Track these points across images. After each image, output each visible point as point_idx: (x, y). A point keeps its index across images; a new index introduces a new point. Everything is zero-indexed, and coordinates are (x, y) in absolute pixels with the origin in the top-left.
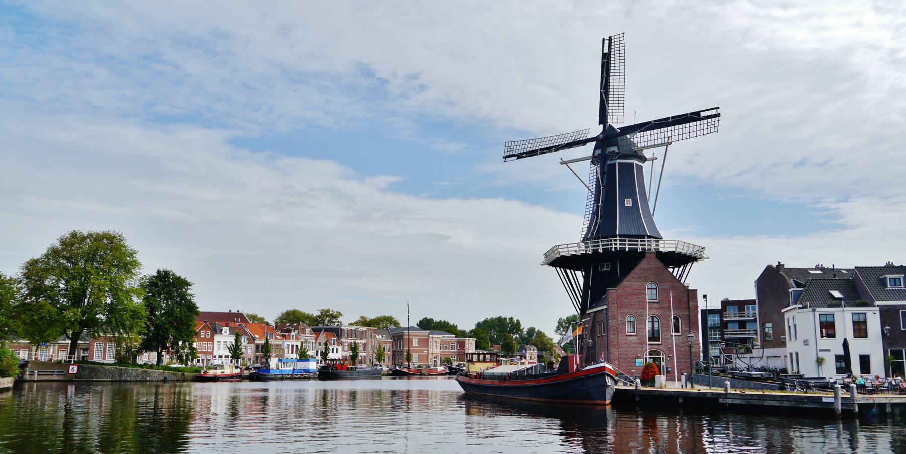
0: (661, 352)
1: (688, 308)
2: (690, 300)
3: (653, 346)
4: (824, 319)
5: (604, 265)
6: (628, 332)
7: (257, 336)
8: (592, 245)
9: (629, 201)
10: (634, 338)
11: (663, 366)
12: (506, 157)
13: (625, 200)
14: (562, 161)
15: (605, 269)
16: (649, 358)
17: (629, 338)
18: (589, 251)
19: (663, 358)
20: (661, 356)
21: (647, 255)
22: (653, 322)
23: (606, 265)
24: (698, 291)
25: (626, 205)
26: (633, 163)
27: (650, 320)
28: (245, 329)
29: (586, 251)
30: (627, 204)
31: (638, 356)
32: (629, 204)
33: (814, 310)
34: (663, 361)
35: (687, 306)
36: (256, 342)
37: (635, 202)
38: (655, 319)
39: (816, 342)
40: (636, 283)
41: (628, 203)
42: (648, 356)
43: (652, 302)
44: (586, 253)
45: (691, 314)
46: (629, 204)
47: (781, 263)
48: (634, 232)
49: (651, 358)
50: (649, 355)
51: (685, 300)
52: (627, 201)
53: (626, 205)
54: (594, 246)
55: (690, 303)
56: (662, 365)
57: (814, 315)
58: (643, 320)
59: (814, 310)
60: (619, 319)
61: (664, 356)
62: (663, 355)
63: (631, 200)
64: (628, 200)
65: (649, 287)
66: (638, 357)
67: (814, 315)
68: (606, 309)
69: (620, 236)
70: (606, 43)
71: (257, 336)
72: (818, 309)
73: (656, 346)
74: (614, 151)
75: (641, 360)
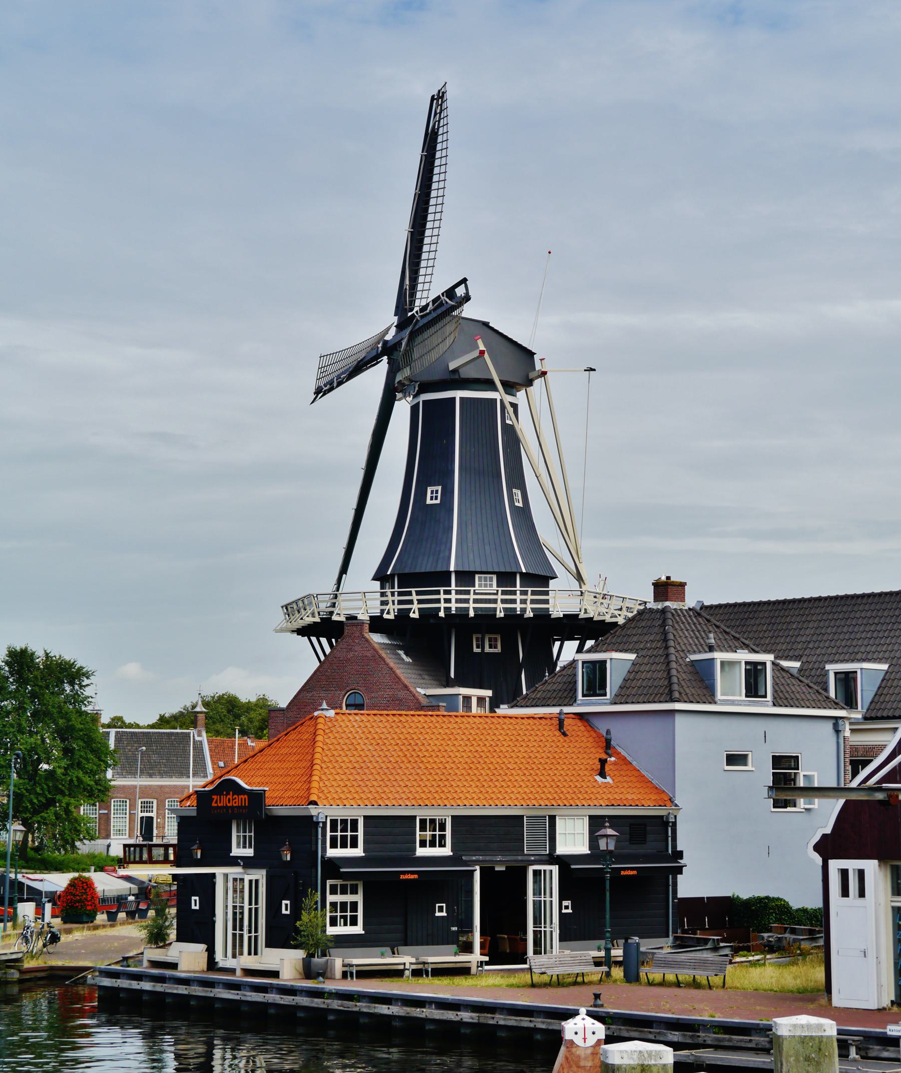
8: (397, 598)
9: (437, 492)
13: (429, 490)
18: (388, 613)
26: (454, 399)
29: (382, 611)
30: (432, 499)
32: (436, 498)
37: (447, 493)
41: (433, 496)
44: (381, 617)
46: (436, 498)
48: (426, 566)
52: (432, 492)
53: (429, 502)
54: (400, 602)
63: (439, 488)
64: (434, 488)
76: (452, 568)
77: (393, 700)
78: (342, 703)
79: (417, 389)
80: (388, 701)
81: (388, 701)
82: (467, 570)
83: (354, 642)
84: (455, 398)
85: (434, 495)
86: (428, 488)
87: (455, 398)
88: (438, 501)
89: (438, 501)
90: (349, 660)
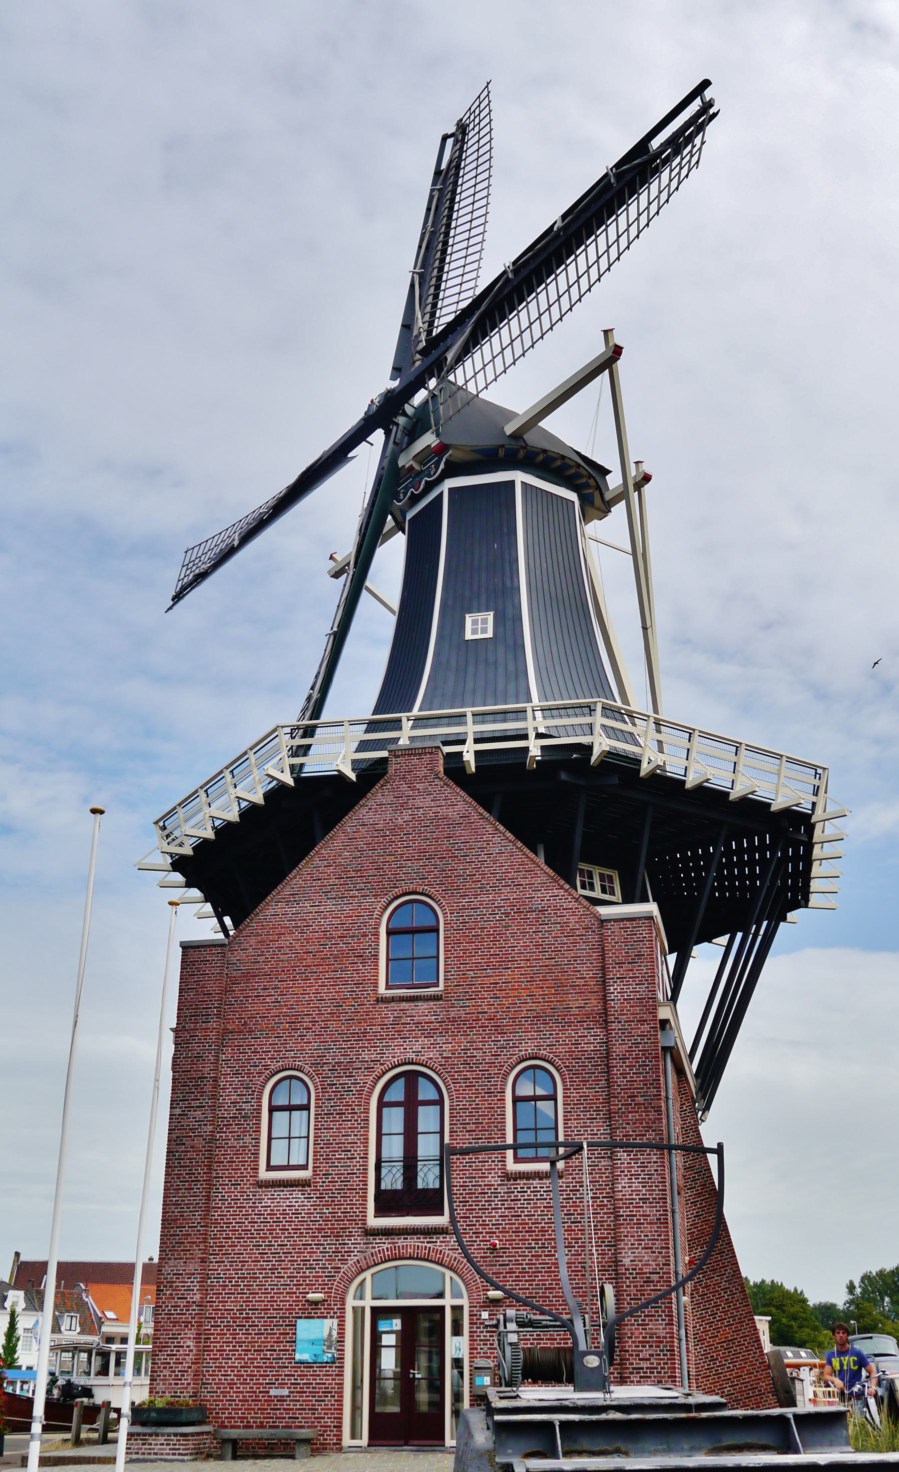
0: (448, 1274)
1: (604, 1018)
2: (614, 973)
3: (401, 1242)
6: (269, 1168)
7: (110, 1315)
9: (485, 621)
10: (297, 1197)
11: (458, 1363)
12: (178, 597)
13: (469, 619)
14: (332, 564)
16: (373, 1309)
17: (268, 1198)
19: (458, 1310)
20: (448, 1302)
22: (411, 1105)
26: (513, 482)
27: (397, 1093)
28: (84, 1295)
30: (474, 632)
31: (316, 1303)
34: (457, 1331)
35: (594, 1004)
36: (104, 1329)
38: (425, 1092)
40: (330, 905)
43: (402, 999)
45: (618, 1049)
46: (484, 631)
50: (442, 1309)
51: (588, 971)
52: (475, 622)
53: (469, 636)
55: (614, 990)
56: (450, 1353)
58: (350, 1098)
60: (228, 1096)
61: (464, 1302)
62: (456, 1295)
63: (490, 616)
64: (479, 616)
65: (396, 924)
66: (314, 1310)
70: (450, 142)
71: (110, 1315)
73: (412, 1242)
74: (429, 446)
75: (325, 1327)
77: (519, 912)
78: (378, 924)
79: (442, 466)
80: (507, 914)
81: (507, 914)
84: (514, 481)
86: (467, 616)
87: (514, 481)
88: (490, 634)
89: (490, 634)
90: (401, 828)
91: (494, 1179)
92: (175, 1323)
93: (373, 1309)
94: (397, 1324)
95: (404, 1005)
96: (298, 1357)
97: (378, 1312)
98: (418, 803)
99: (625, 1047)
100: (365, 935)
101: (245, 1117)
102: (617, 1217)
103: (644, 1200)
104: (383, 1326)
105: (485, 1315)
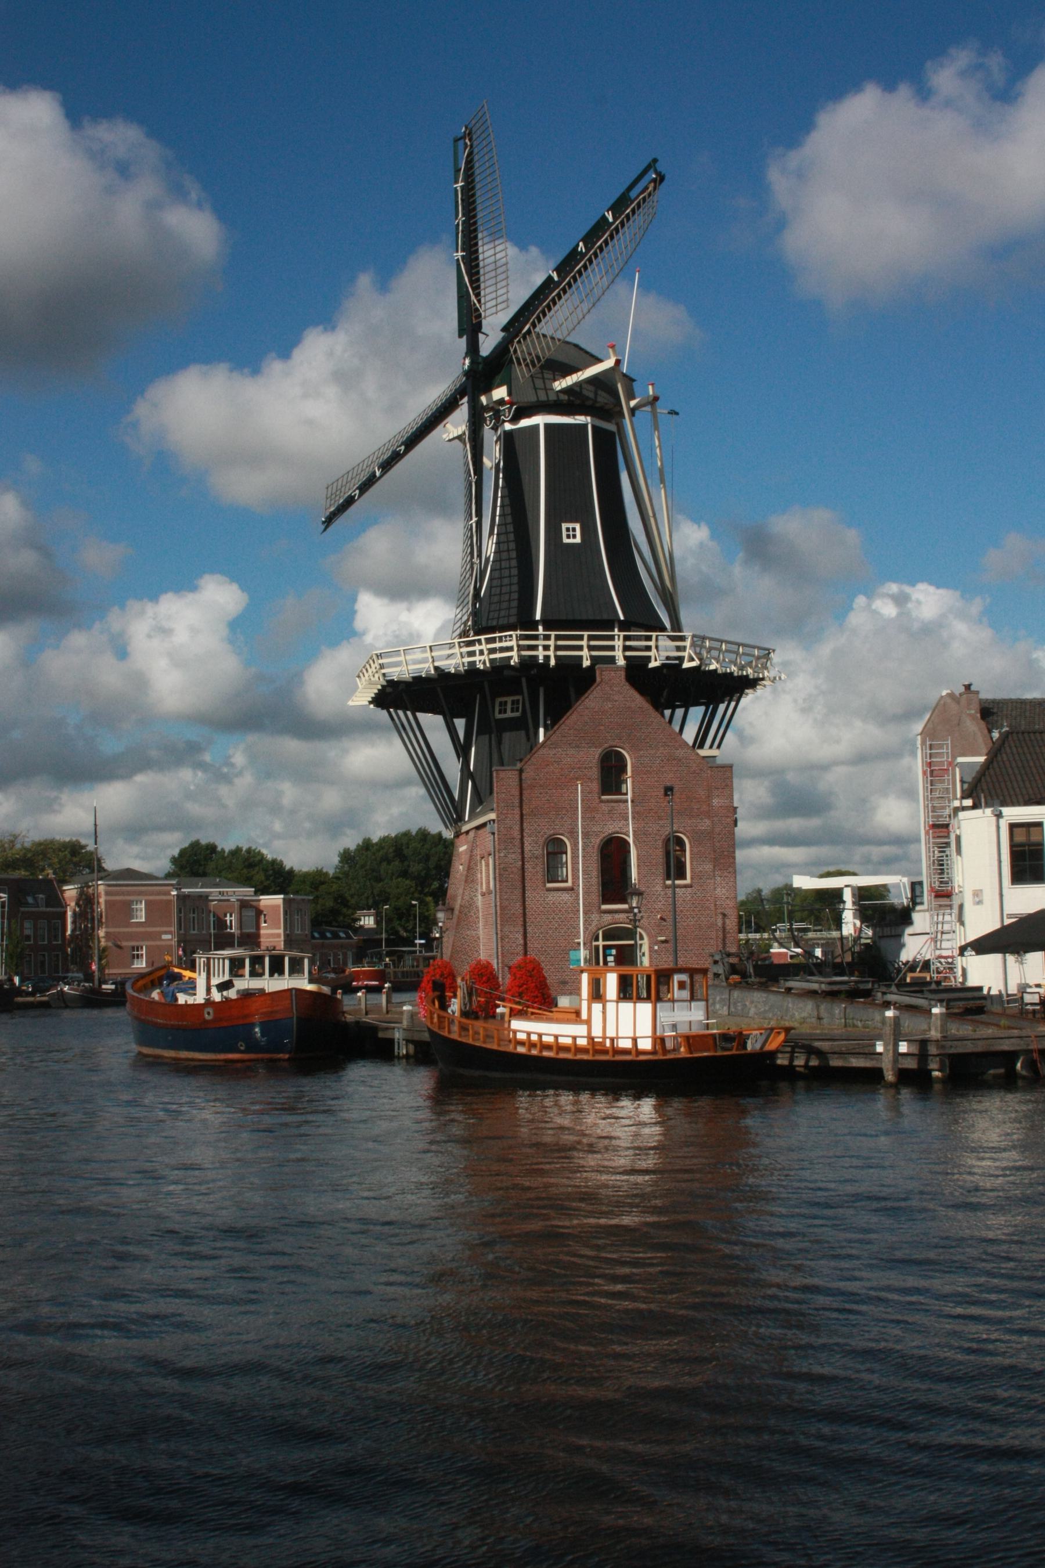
3: (617, 916)
4: (1020, 838)
5: (506, 702)
9: (574, 530)
13: (564, 526)
15: (509, 714)
17: (552, 897)
21: (602, 674)
23: (513, 702)
24: (734, 768)
25: (566, 541)
33: (999, 816)
39: (1001, 895)
40: (571, 751)
41: (572, 534)
42: (601, 943)
46: (574, 536)
47: (973, 688)
49: (610, 947)
52: (568, 529)
55: (715, 802)
57: (998, 827)
59: (999, 816)
63: (578, 526)
64: (571, 526)
67: (998, 827)
68: (494, 821)
69: (549, 624)
72: (1006, 811)
76: (622, 618)
81: (663, 761)
82: (591, 618)
83: (613, 690)
85: (571, 533)
91: (659, 888)
92: (512, 954)
93: (605, 947)
94: (614, 952)
95: (613, 804)
96: (571, 967)
97: (605, 947)
98: (616, 698)
99: (719, 829)
100: (591, 768)
101: (537, 858)
102: (716, 905)
103: (727, 898)
104: (608, 952)
105: (656, 948)
